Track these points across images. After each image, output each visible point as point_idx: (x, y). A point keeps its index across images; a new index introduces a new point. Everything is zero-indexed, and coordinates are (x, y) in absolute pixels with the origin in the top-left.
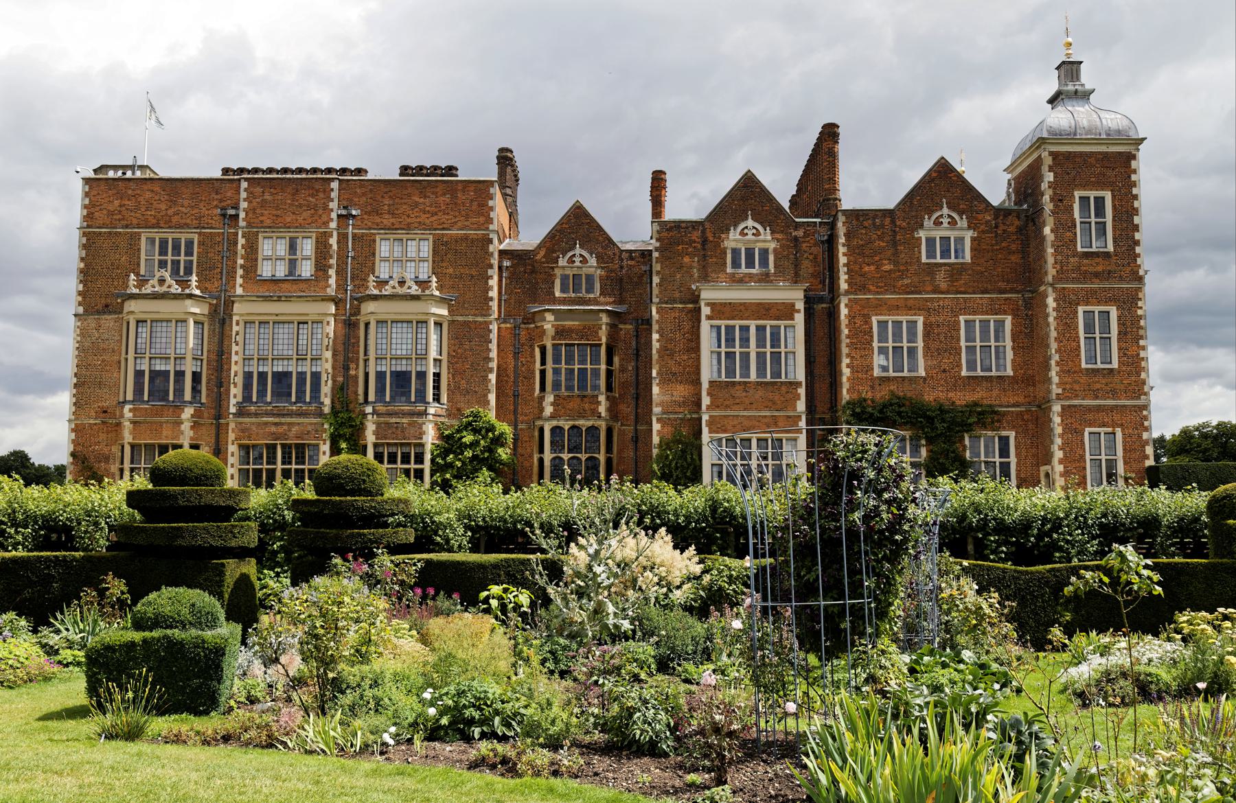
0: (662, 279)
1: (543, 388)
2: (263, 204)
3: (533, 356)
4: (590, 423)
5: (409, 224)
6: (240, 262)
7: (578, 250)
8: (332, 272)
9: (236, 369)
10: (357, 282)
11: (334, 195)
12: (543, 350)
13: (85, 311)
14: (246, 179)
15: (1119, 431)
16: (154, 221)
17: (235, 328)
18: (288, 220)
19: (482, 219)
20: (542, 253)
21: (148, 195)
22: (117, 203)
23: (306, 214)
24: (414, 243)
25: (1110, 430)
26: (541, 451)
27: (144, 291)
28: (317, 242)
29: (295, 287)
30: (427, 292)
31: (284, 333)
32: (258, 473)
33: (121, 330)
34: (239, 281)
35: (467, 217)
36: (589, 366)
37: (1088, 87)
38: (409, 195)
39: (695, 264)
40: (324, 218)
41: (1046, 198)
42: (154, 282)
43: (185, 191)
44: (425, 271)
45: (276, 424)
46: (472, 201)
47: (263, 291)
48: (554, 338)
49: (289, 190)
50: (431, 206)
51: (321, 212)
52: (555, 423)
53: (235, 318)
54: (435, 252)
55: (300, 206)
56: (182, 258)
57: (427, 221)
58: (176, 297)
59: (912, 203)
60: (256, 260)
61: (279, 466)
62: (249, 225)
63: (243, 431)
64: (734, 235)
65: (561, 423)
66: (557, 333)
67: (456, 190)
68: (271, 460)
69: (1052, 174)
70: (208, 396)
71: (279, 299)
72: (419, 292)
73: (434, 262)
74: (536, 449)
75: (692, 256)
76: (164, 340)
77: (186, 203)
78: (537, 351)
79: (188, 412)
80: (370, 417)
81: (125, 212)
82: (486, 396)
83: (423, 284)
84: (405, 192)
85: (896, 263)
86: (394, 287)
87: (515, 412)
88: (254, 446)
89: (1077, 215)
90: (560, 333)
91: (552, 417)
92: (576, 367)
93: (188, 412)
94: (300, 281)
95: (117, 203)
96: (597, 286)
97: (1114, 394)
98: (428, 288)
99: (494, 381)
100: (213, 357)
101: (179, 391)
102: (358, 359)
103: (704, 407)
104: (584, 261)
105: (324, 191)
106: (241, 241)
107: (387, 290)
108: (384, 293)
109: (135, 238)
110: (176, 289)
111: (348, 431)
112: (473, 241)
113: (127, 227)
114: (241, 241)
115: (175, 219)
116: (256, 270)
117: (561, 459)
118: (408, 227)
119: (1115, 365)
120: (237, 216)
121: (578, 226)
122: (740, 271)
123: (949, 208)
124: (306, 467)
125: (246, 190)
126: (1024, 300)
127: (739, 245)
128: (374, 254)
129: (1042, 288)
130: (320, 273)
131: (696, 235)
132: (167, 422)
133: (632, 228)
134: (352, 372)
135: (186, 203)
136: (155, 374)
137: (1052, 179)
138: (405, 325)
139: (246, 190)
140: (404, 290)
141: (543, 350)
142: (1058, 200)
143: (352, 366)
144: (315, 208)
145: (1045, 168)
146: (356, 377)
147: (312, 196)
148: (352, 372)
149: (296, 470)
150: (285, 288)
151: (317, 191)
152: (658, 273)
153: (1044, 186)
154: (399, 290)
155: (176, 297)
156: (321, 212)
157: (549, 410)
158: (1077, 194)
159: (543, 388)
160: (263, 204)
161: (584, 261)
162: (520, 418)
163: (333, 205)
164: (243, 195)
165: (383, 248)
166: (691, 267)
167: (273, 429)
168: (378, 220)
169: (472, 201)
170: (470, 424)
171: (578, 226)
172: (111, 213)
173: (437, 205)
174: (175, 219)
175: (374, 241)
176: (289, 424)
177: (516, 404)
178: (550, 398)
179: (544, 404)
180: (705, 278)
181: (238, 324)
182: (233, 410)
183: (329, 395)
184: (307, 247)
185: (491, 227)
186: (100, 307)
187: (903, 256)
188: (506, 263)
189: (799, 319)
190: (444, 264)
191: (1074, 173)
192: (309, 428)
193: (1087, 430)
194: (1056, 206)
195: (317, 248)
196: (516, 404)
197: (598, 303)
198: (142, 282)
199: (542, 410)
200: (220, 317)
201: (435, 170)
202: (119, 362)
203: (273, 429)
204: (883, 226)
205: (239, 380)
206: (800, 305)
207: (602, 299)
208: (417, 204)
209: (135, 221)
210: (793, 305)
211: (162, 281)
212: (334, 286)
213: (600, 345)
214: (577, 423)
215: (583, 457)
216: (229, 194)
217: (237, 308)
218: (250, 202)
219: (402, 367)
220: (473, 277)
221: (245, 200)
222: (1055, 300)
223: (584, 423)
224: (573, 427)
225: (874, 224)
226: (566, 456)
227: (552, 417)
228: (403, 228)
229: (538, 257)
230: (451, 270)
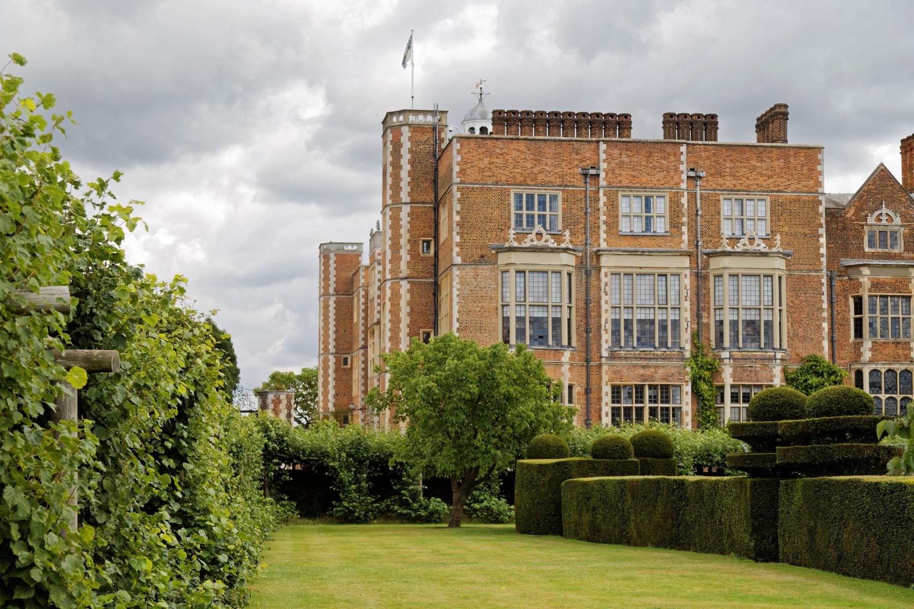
1: (859, 333)
2: (621, 165)
3: (847, 306)
4: (904, 367)
5: (748, 186)
6: (603, 218)
7: (884, 210)
8: (685, 229)
9: (607, 316)
10: (705, 239)
11: (683, 158)
12: (859, 302)
13: (464, 260)
14: (604, 142)
16: (522, 178)
17: (604, 280)
18: (644, 180)
19: (812, 183)
20: (852, 211)
21: (515, 154)
22: (487, 160)
23: (660, 176)
27: (524, 245)
28: (671, 201)
29: (652, 242)
31: (643, 285)
32: (628, 410)
33: (496, 279)
34: (603, 236)
35: (799, 180)
36: (901, 316)
38: (748, 160)
40: (676, 179)
42: (745, 240)
43: (548, 151)
45: (644, 367)
46: (802, 166)
47: (625, 245)
48: (870, 291)
49: (644, 152)
50: (767, 169)
51: (672, 173)
52: (873, 367)
53: (603, 270)
54: (773, 212)
55: (654, 168)
56: (524, 212)
57: (764, 184)
58: (553, 250)
60: (617, 216)
61: (647, 405)
62: (610, 185)
63: (615, 373)
65: (878, 367)
66: (873, 286)
67: (789, 155)
68: (640, 399)
70: (578, 340)
71: (643, 253)
72: (766, 250)
76: (536, 290)
77: (549, 162)
78: (851, 302)
79: (566, 356)
80: (727, 361)
81: (494, 169)
82: (820, 342)
84: (744, 156)
86: (744, 245)
88: (625, 386)
90: (876, 285)
91: (871, 361)
92: (890, 316)
93: (566, 356)
94: (655, 236)
95: (487, 160)
96: (901, 242)
98: (563, 241)
100: (582, 305)
101: (557, 337)
102: (709, 309)
104: (890, 219)
105: (675, 155)
106: (603, 199)
107: (739, 248)
109: (504, 194)
110: (552, 243)
111: (707, 374)
113: (497, 183)
114: (603, 199)
115: (540, 177)
116: (617, 227)
117: (895, 399)
118: (748, 191)
120: (598, 175)
124: (670, 405)
125: (605, 152)
128: (719, 213)
130: (675, 230)
132: (550, 364)
134: (705, 320)
135: (549, 162)
136: (534, 321)
139: (605, 152)
141: (859, 302)
143: (705, 314)
144: (667, 170)
146: (708, 324)
147: (664, 158)
148: (705, 320)
149: (662, 408)
150: (640, 244)
151: (669, 154)
154: (750, 248)
155: (553, 250)
156: (672, 173)
157: (867, 355)
159: (859, 333)
160: (621, 165)
161: (890, 219)
163: (683, 168)
164: (603, 156)
167: (642, 371)
168: (721, 181)
169: (802, 166)
170: (811, 368)
172: (481, 170)
174: (540, 177)
175: (719, 201)
176: (656, 367)
178: (867, 344)
179: (862, 349)
181: (606, 276)
182: (605, 354)
183: (689, 341)
184: (660, 206)
186: (476, 258)
190: (781, 223)
192: (673, 371)
195: (671, 207)
197: (902, 258)
198: (521, 236)
199: (860, 355)
200: (589, 266)
202: (497, 309)
203: (642, 371)
205: (609, 326)
207: (906, 255)
208: (755, 167)
209: (504, 178)
211: (539, 235)
212: (686, 242)
214: (892, 367)
215: (899, 397)
216: (588, 155)
217: (604, 261)
218: (609, 163)
219: (752, 316)
220: (806, 235)
221: (604, 161)
223: (898, 367)
224: (889, 370)
227: (871, 361)
229: (849, 215)
230: (786, 229)
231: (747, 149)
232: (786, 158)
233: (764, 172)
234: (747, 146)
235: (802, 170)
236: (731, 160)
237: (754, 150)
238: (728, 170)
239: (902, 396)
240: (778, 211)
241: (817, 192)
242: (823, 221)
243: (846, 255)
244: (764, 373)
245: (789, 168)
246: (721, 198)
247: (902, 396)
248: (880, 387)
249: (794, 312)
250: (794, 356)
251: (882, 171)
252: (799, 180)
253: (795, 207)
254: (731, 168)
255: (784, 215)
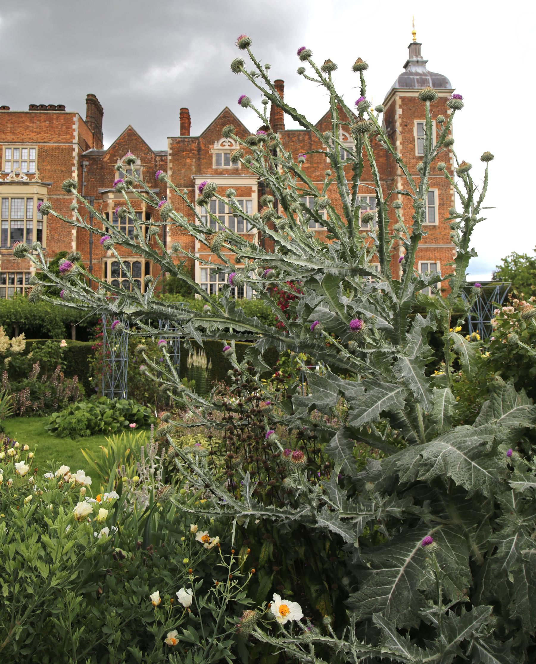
0: (173, 173)
4: (135, 260)
5: (23, 139)
15: (438, 263)
19: (68, 136)
20: (108, 157)
24: (26, 151)
25: (433, 262)
26: (106, 277)
30: (33, 180)
35: (59, 135)
37: (425, 59)
38: (23, 122)
39: (193, 164)
41: (398, 124)
44: (33, 168)
50: (37, 128)
54: (40, 156)
57: (34, 138)
59: (321, 127)
64: (217, 146)
67: (52, 119)
69: (401, 110)
73: (38, 162)
74: (103, 275)
75: (191, 158)
83: (30, 175)
84: (21, 120)
85: (311, 163)
87: (91, 253)
89: (415, 134)
97: (436, 241)
99: (75, 234)
103: (196, 250)
108: (6, 181)
112: (62, 150)
117: (117, 281)
118: (22, 142)
119: (437, 223)
121: (130, 140)
122: (220, 167)
123: (343, 130)
126: (387, 185)
127: (220, 152)
129: (396, 178)
131: (194, 146)
133: (159, 143)
137: (401, 113)
138: (20, 200)
140: (19, 179)
142: (404, 125)
145: (397, 106)
152: (171, 169)
153: (397, 117)
158: (416, 122)
162: (93, 257)
165: (7, 154)
166: (191, 165)
169: (62, 125)
171: (130, 140)
173: (41, 128)
175: (2, 149)
177: (91, 248)
180: (199, 172)
185: (74, 141)
187: (315, 158)
188: (86, 163)
189: (255, 196)
190: (45, 164)
191: (414, 109)
193: (420, 262)
194: (403, 129)
196: (91, 248)
201: (52, 107)
204: (304, 140)
206: (255, 188)
208: (28, 127)
210: (251, 188)
213: (142, 212)
214: (127, 259)
220: (62, 171)
222: (402, 185)
225: (299, 139)
226: (121, 279)
228: (20, 142)
229: (105, 159)
230: (49, 167)
231: (23, 115)
232: (51, 120)
233: (35, 130)
234: (23, 113)
235: (61, 128)
236: (11, 123)
237: (28, 116)
238: (9, 129)
239: (123, 279)
240: (43, 156)
241: (72, 142)
242: (75, 162)
243: (103, 186)
244: (24, 265)
245: (52, 127)
246: (4, 148)
247: (123, 279)
248: (119, 273)
249: (52, 223)
250: (51, 253)
251: (130, 130)
252: (59, 135)
253: (56, 153)
254: (11, 128)
255: (48, 158)
